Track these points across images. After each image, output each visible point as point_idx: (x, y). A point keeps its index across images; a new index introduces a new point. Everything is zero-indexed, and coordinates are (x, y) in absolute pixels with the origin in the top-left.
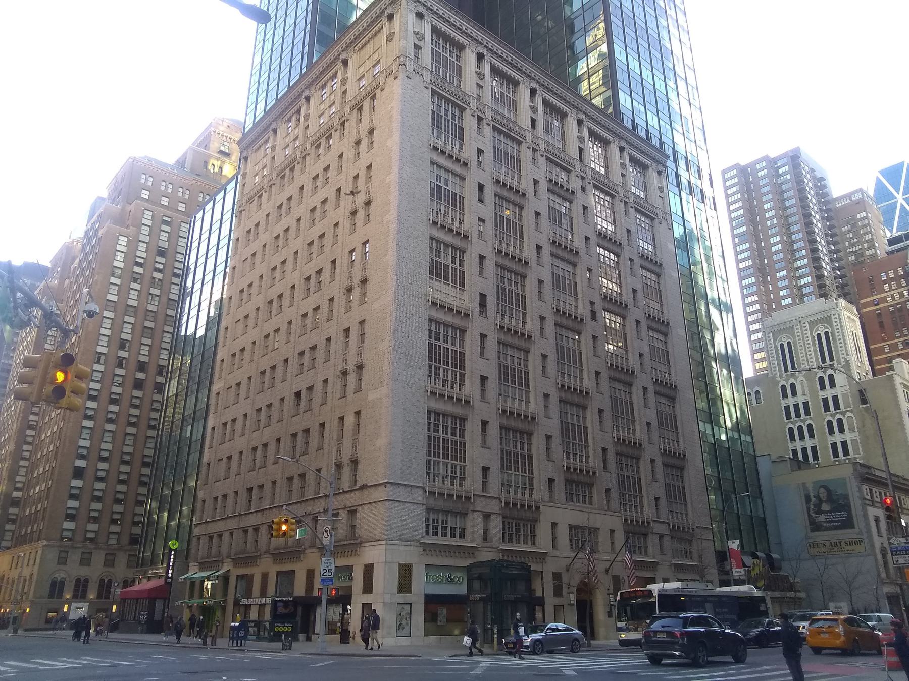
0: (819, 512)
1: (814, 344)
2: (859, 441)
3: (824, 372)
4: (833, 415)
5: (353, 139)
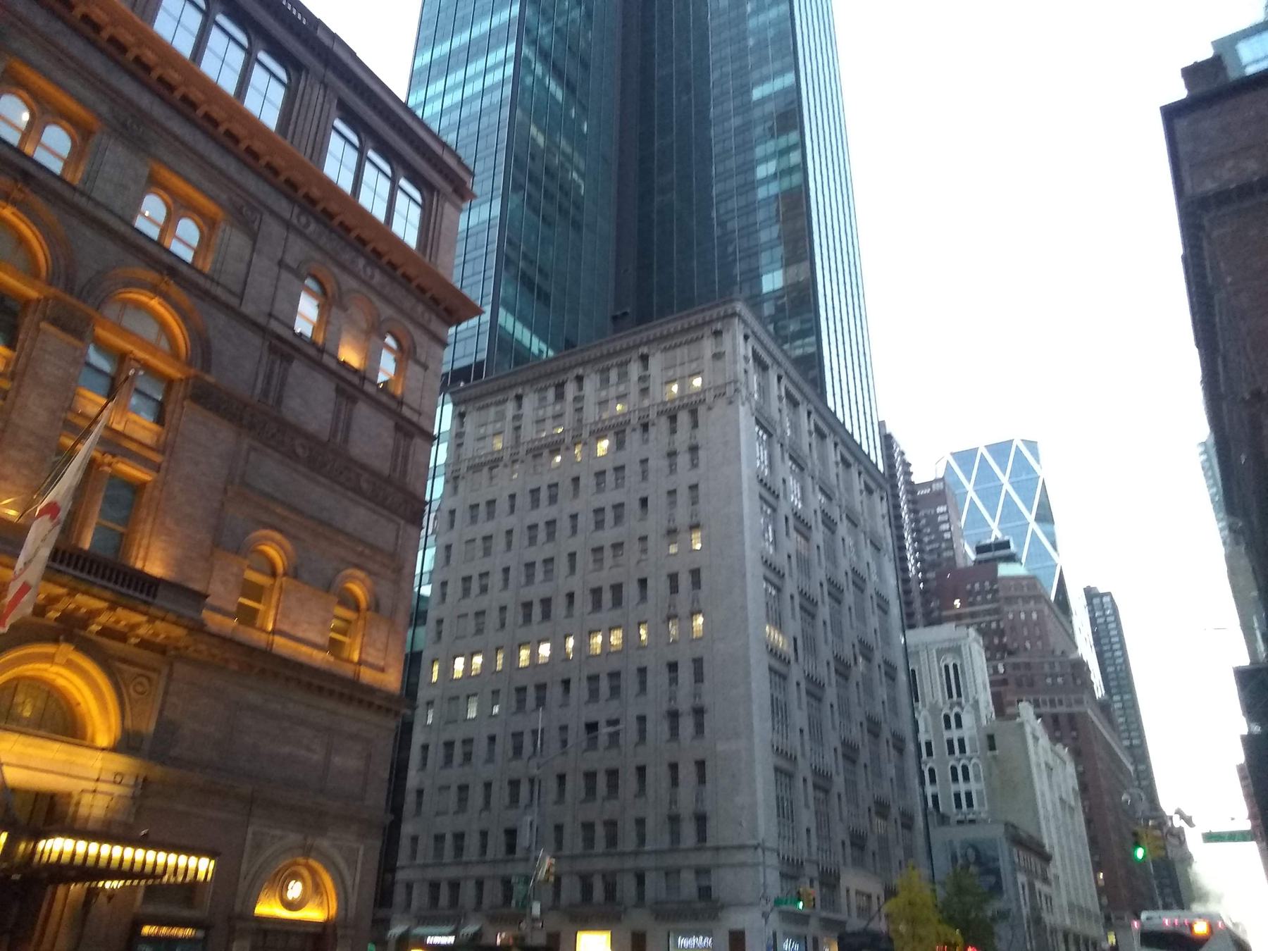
1: (941, 675)
2: (985, 793)
5: (666, 449)
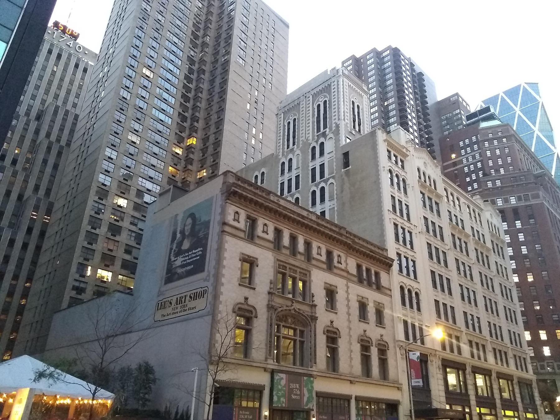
0: (179, 253)
1: (313, 115)
2: (336, 209)
3: (317, 142)
4: (317, 186)
